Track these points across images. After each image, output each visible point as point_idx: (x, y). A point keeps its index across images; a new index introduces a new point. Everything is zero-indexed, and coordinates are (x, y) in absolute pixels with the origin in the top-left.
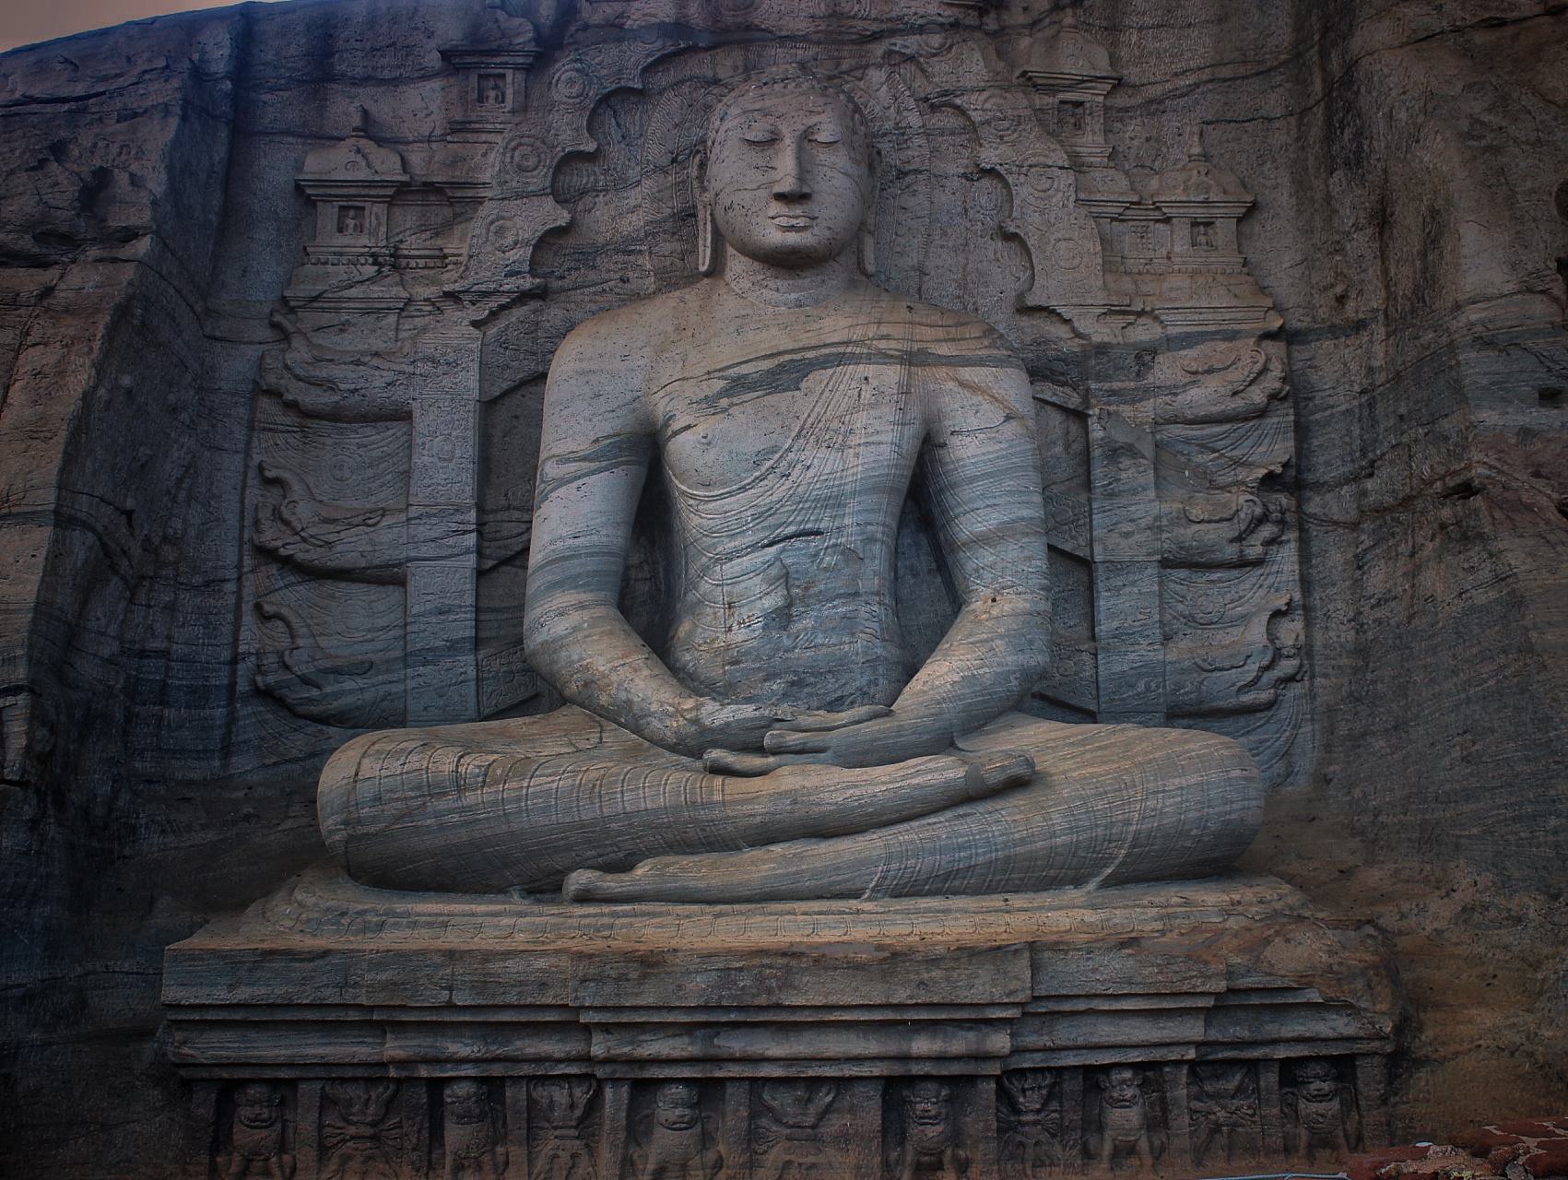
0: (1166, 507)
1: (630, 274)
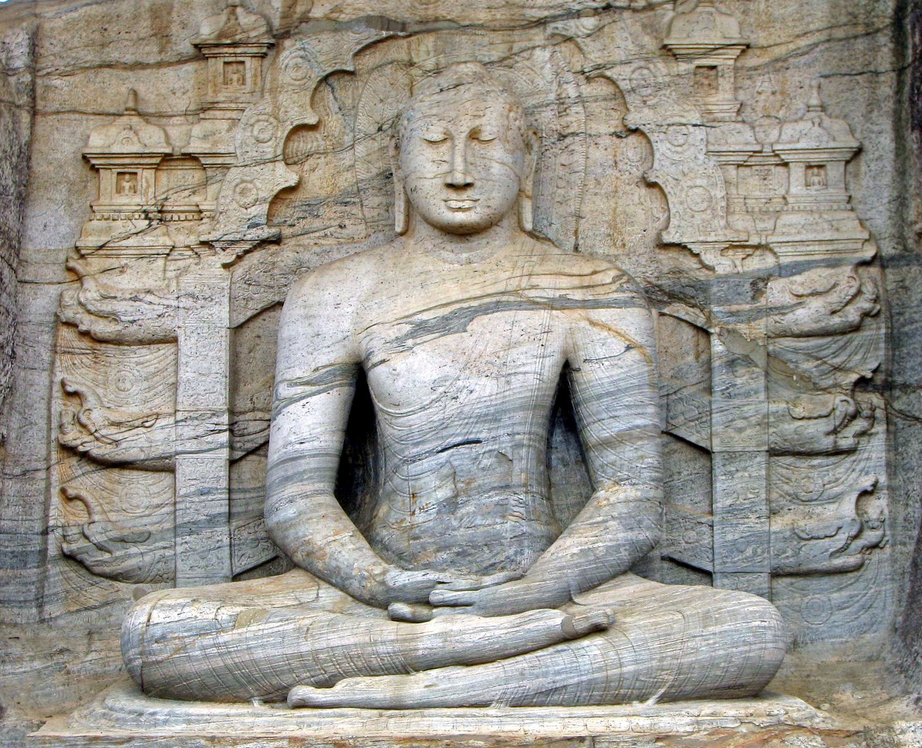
0: (773, 407)
1: (347, 222)
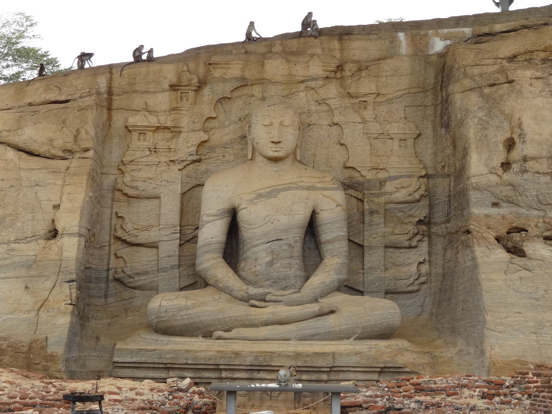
0: (387, 230)
1: (226, 155)
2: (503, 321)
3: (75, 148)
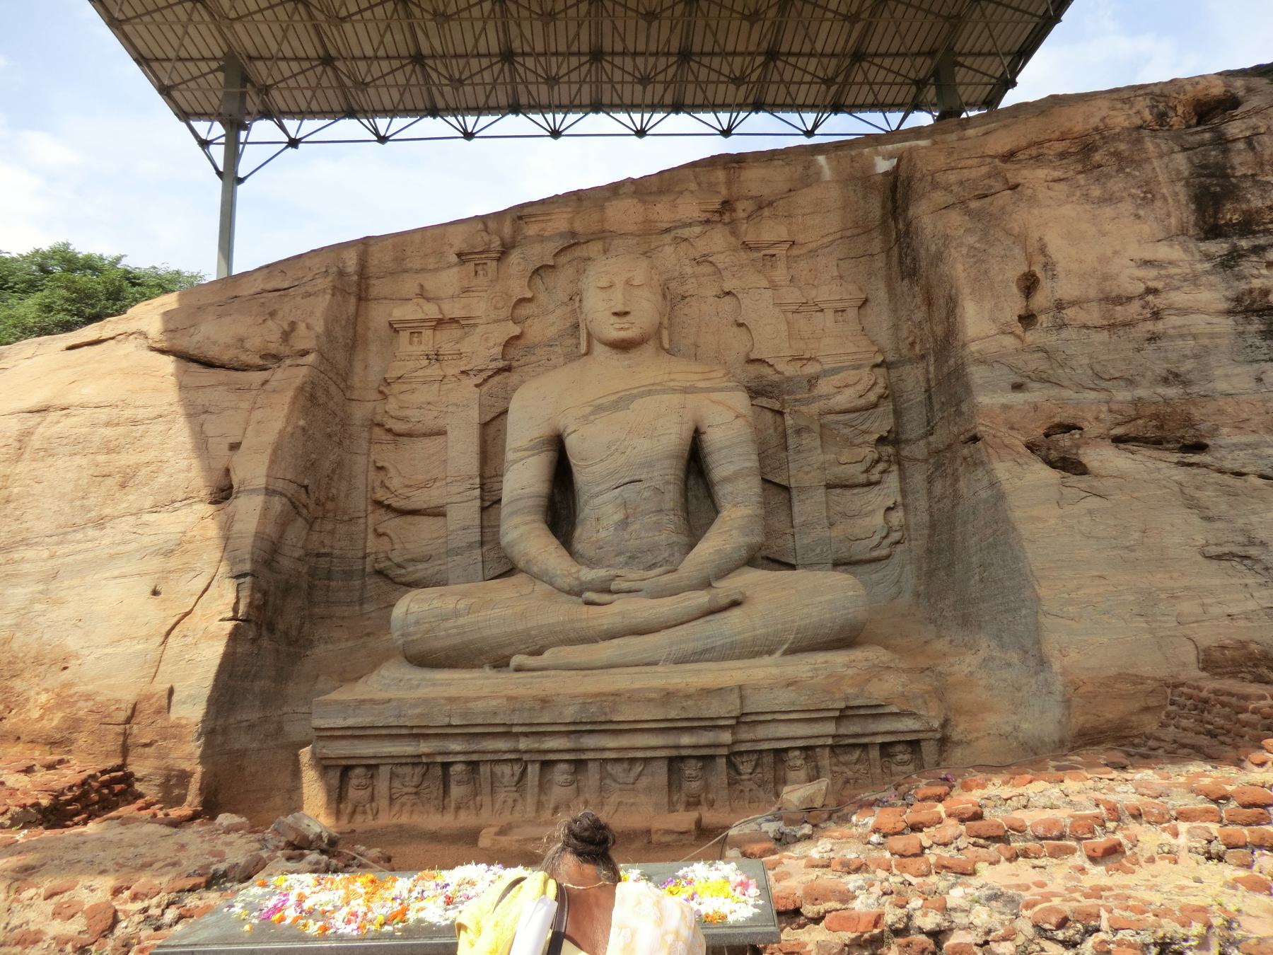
0: (828, 457)
2: (1073, 595)
3: (284, 350)
